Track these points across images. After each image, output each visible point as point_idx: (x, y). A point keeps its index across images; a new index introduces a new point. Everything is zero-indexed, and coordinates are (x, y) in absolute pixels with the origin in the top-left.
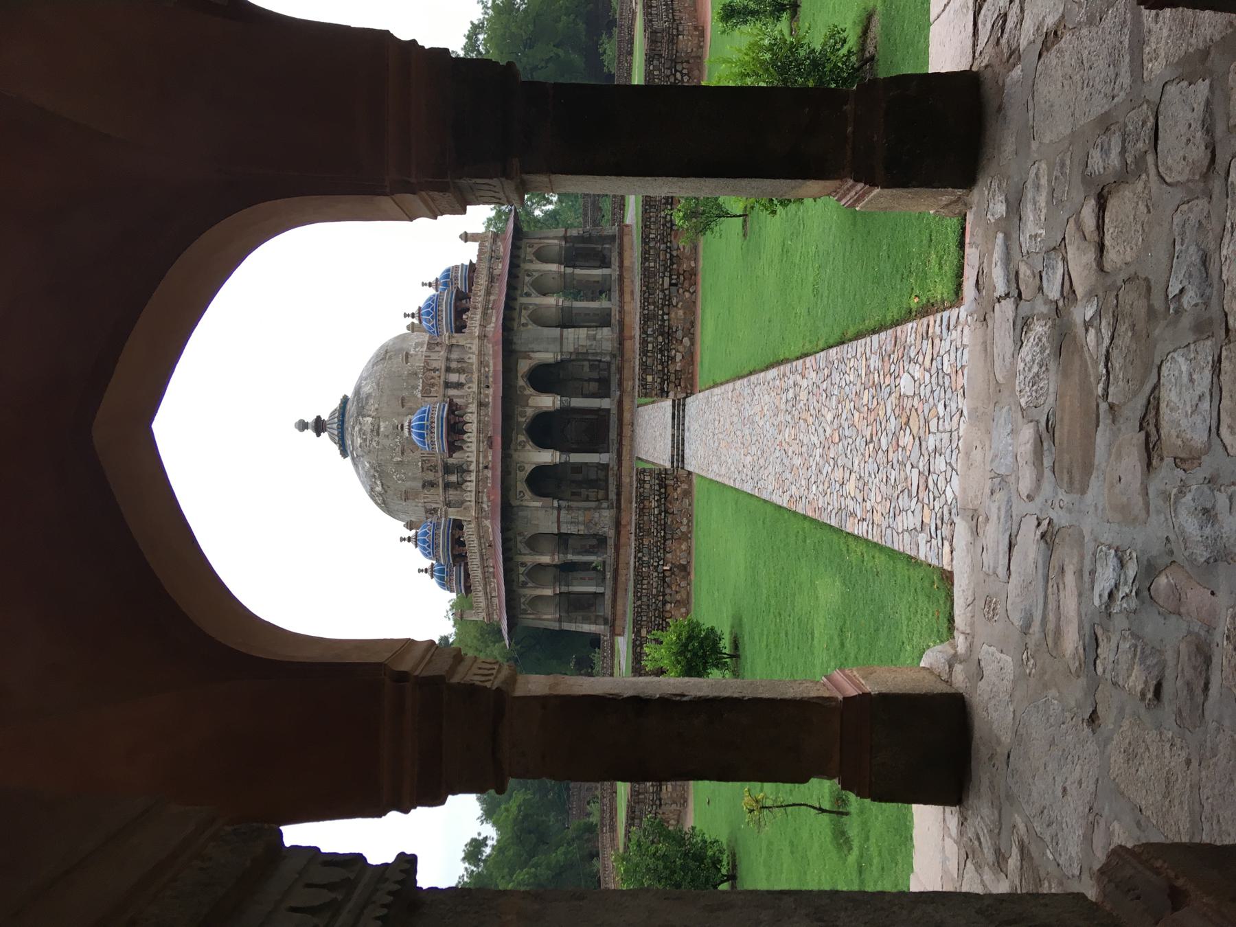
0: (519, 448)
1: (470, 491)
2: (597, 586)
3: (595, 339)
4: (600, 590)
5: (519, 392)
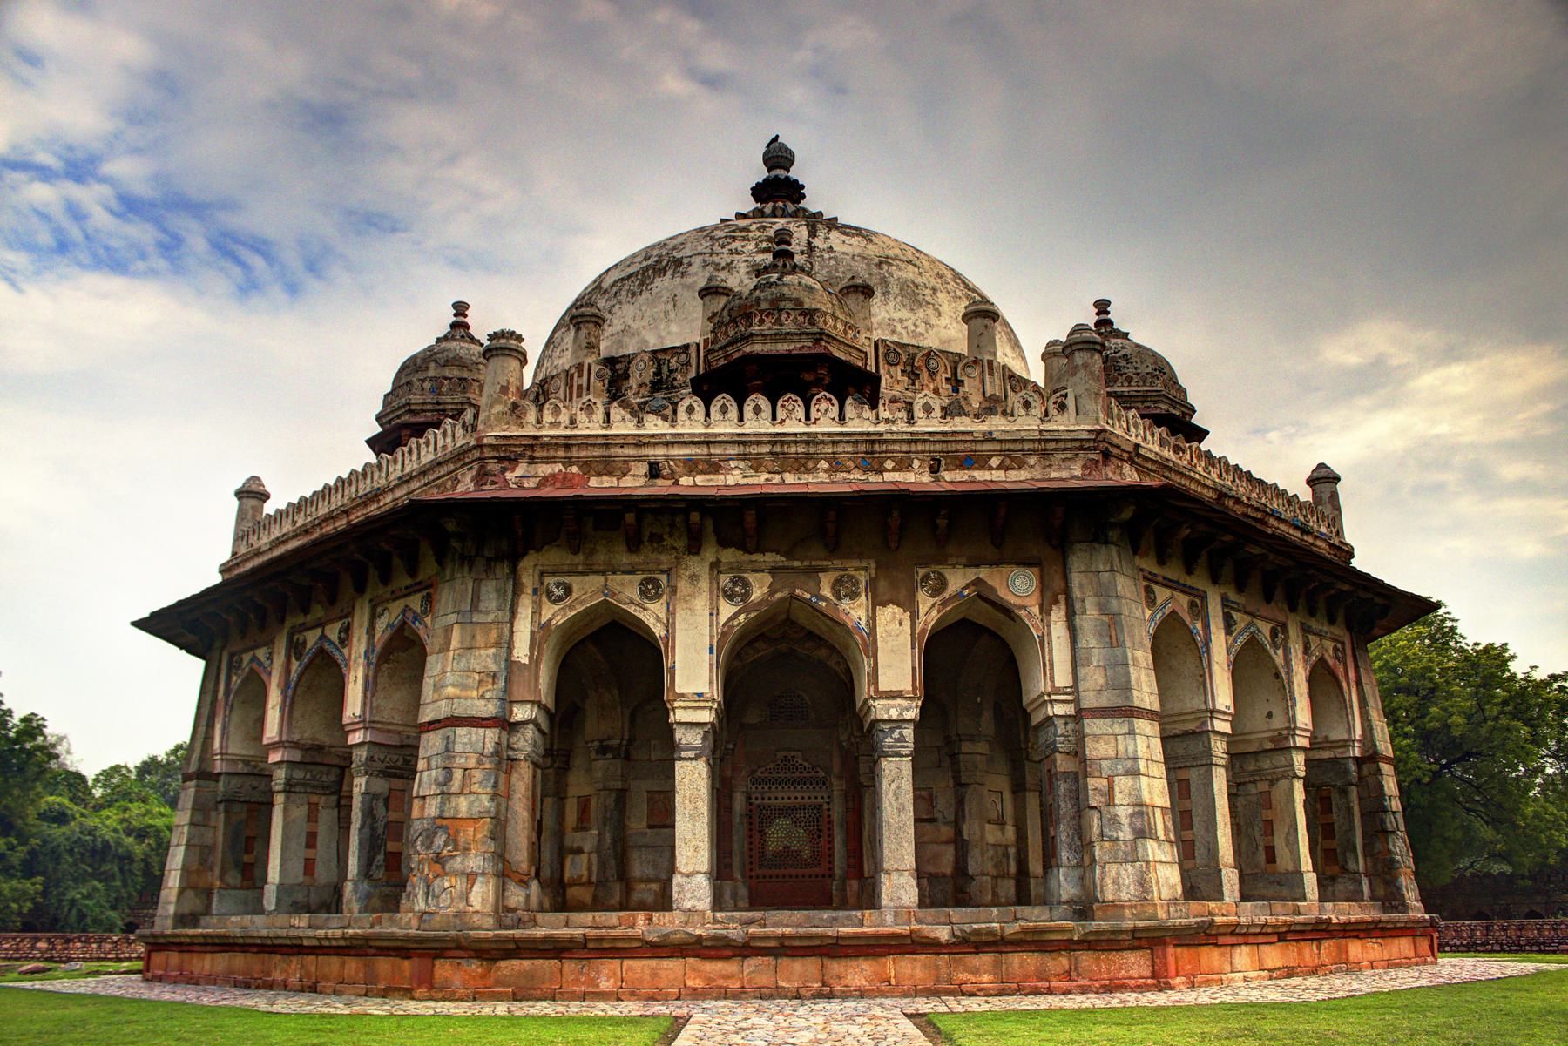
0: (725, 580)
1: (573, 422)
2: (281, 887)
4: (270, 899)
5: (922, 571)
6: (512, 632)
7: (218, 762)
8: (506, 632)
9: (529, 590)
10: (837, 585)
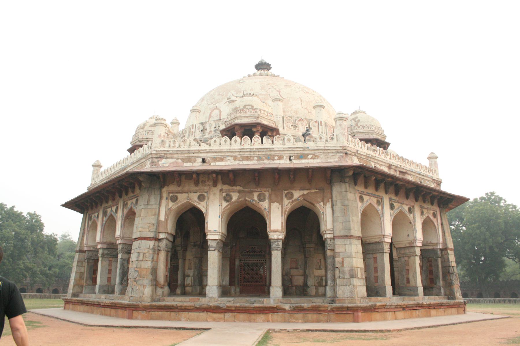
0: (224, 194)
1: (180, 146)
2: (100, 286)
3: (352, 276)
5: (286, 192)
6: (159, 211)
7: (85, 247)
8: (157, 210)
9: (165, 198)
10: (259, 196)
